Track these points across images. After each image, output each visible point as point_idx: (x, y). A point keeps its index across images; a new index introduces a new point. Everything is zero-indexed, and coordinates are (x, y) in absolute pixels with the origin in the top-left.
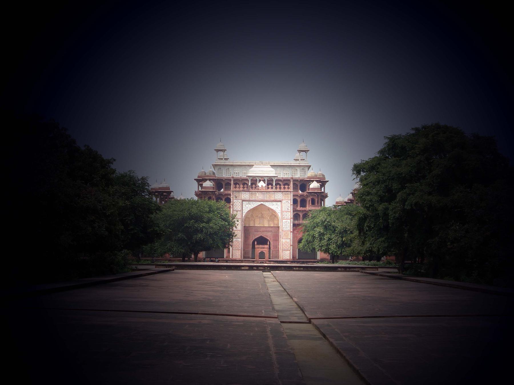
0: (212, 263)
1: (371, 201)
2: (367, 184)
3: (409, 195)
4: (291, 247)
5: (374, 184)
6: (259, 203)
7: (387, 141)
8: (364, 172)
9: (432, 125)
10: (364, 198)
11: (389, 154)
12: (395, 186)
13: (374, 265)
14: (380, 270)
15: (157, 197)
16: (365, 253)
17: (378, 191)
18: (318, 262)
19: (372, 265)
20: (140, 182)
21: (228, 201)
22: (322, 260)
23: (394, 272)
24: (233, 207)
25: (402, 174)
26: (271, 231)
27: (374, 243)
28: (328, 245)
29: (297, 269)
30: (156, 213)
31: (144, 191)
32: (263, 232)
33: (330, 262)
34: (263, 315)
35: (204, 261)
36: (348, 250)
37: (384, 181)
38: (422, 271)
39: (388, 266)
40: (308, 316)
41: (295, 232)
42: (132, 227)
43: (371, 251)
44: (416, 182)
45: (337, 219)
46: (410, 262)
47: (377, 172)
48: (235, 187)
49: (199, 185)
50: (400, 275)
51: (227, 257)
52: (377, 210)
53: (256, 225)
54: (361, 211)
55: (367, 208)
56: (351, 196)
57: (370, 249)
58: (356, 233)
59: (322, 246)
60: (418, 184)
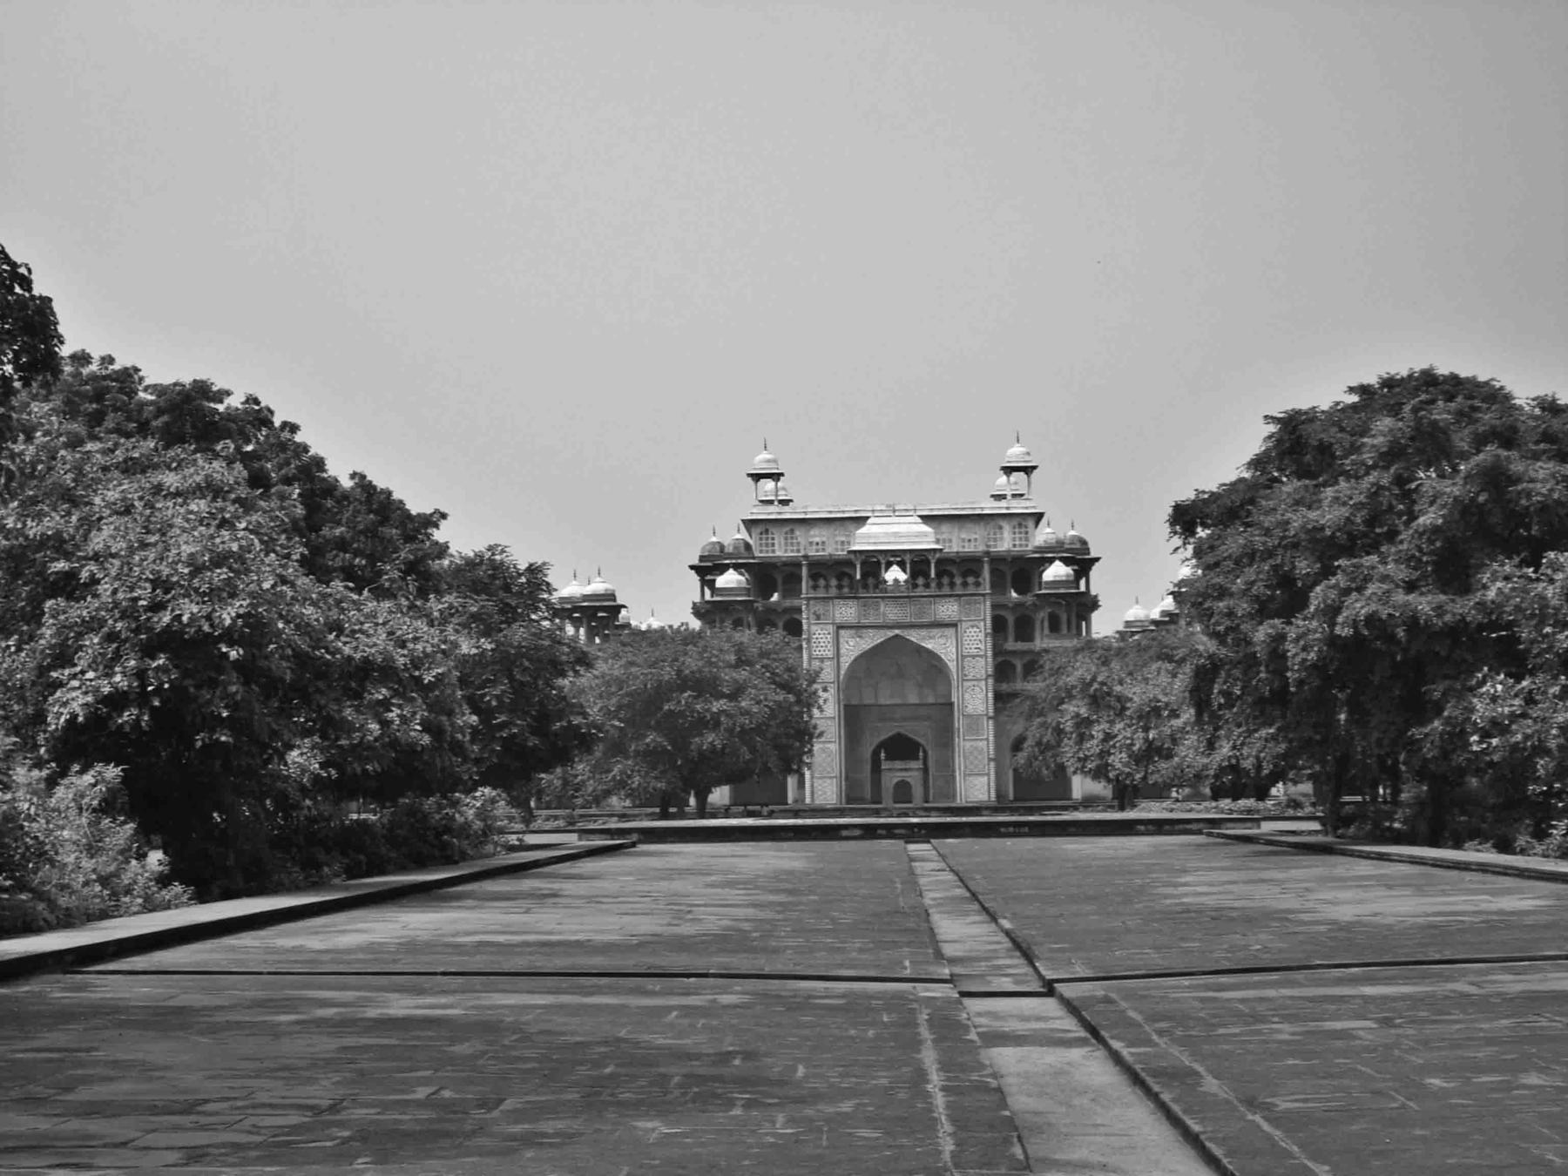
0: (749, 822)
1: (1230, 614)
2: (1217, 564)
3: (1346, 592)
4: (992, 764)
5: (1237, 562)
6: (891, 633)
7: (1273, 428)
8: (1205, 526)
9: (1410, 376)
10: (1209, 608)
11: (1280, 470)
12: (1304, 566)
13: (1249, 811)
14: (1267, 827)
15: (577, 623)
16: (1216, 777)
17: (1253, 583)
18: (1075, 808)
19: (1241, 812)
20: (523, 580)
21: (794, 628)
22: (1089, 802)
23: (1310, 833)
24: (809, 648)
25: (1322, 528)
26: (928, 718)
27: (1243, 744)
28: (1104, 754)
29: (1011, 829)
30: (576, 672)
31: (536, 609)
32: (905, 719)
33: (1112, 807)
34: (907, 973)
35: (727, 813)
36: (1164, 767)
37: (1270, 554)
38: (1396, 825)
39: (1291, 812)
40: (1044, 972)
41: (1003, 718)
42: (502, 718)
43: (1234, 769)
44: (1368, 554)
45: (1130, 674)
46: (1359, 798)
47: (1247, 525)
48: (815, 587)
49: (704, 583)
50: (1330, 839)
51: (796, 801)
52: (1249, 643)
53: (882, 701)
54: (1201, 648)
55: (1220, 637)
56: (1169, 603)
57: (1234, 761)
58: (1188, 714)
59: (1086, 758)
60: (1374, 558)
